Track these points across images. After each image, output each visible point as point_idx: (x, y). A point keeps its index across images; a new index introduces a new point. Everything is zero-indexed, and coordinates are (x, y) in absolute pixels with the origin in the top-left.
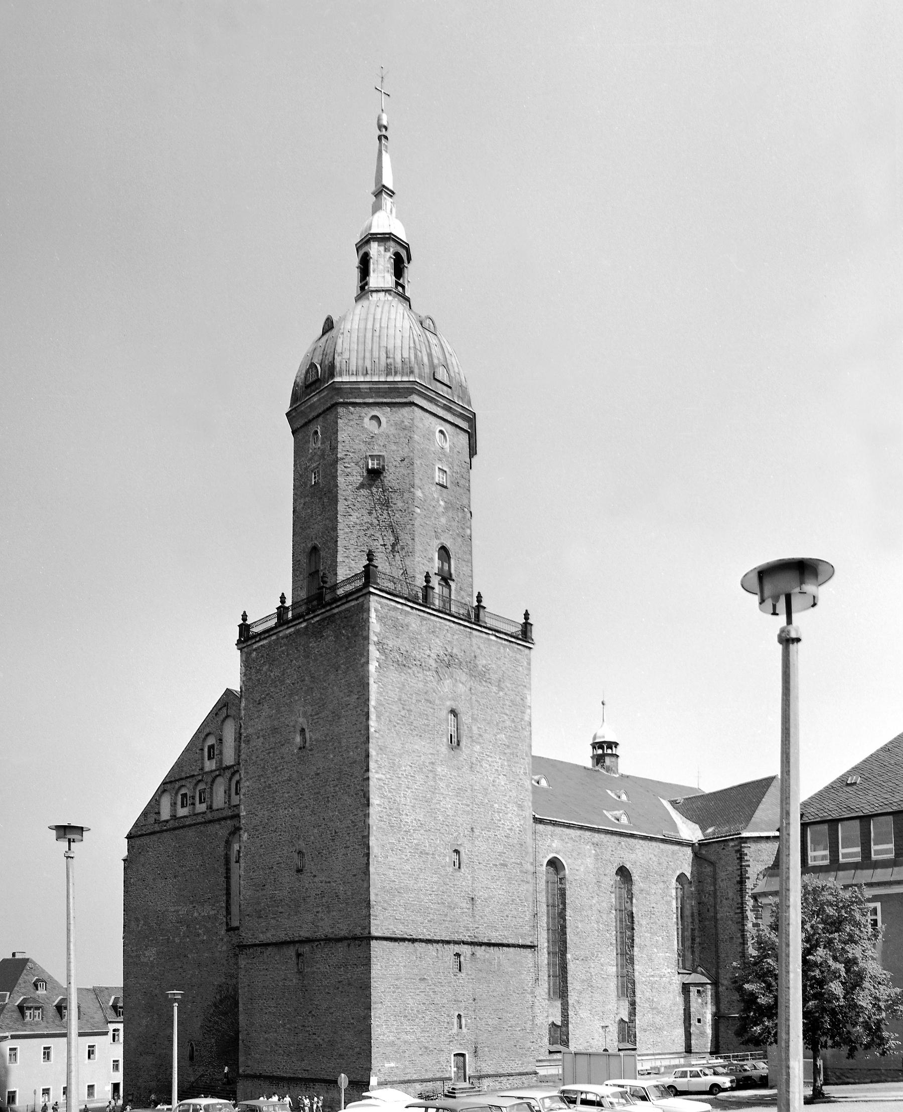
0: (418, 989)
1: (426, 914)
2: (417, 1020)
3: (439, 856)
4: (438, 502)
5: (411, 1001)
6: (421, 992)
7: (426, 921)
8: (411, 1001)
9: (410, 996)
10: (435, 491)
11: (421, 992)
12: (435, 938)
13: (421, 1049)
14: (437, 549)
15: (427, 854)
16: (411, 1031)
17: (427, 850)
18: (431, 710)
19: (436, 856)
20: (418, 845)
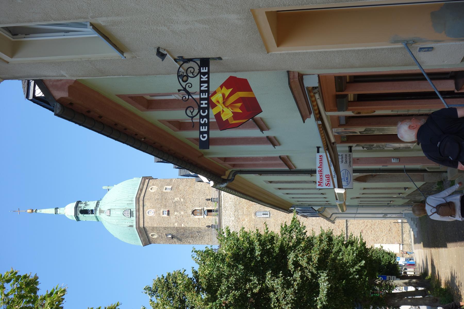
0: (366, 234)
1: (336, 230)
2: (378, 235)
3: (313, 223)
4: (176, 215)
5: (371, 238)
6: (367, 233)
7: (339, 229)
8: (371, 238)
9: (369, 238)
10: (172, 217)
11: (367, 233)
12: (345, 225)
13: (389, 233)
14: (194, 216)
15: (313, 228)
16: (382, 238)
17: (311, 229)
18: (258, 226)
19: (313, 224)
20: (310, 233)
